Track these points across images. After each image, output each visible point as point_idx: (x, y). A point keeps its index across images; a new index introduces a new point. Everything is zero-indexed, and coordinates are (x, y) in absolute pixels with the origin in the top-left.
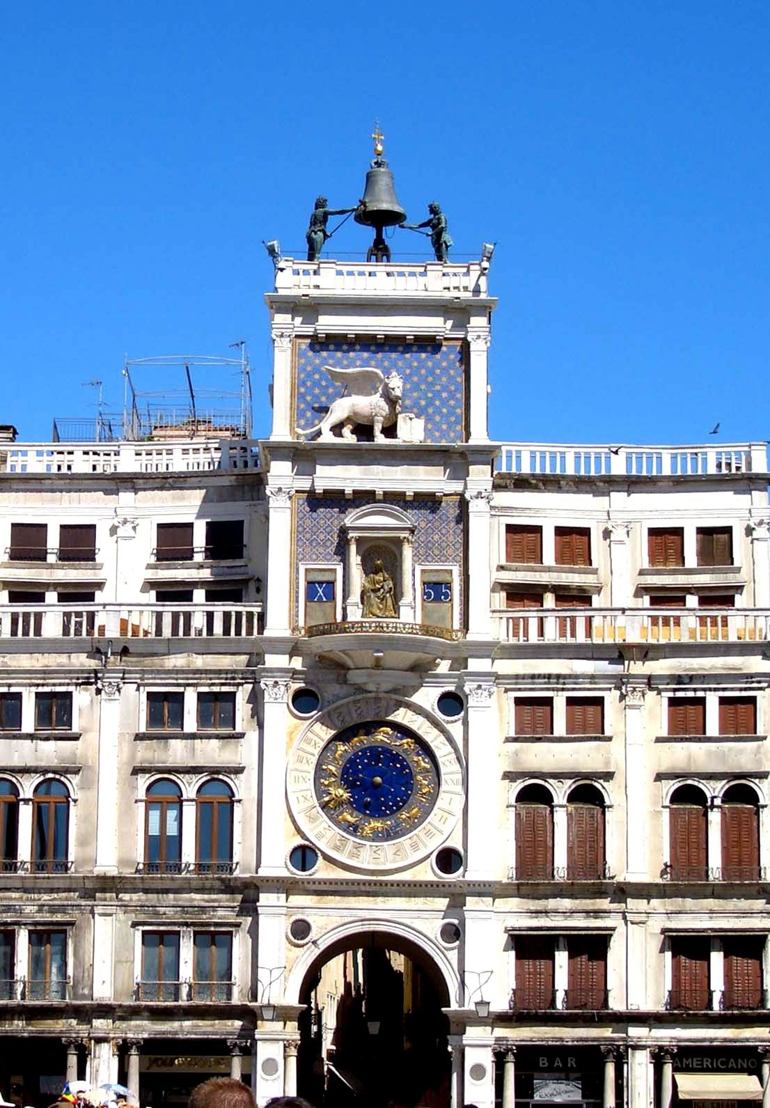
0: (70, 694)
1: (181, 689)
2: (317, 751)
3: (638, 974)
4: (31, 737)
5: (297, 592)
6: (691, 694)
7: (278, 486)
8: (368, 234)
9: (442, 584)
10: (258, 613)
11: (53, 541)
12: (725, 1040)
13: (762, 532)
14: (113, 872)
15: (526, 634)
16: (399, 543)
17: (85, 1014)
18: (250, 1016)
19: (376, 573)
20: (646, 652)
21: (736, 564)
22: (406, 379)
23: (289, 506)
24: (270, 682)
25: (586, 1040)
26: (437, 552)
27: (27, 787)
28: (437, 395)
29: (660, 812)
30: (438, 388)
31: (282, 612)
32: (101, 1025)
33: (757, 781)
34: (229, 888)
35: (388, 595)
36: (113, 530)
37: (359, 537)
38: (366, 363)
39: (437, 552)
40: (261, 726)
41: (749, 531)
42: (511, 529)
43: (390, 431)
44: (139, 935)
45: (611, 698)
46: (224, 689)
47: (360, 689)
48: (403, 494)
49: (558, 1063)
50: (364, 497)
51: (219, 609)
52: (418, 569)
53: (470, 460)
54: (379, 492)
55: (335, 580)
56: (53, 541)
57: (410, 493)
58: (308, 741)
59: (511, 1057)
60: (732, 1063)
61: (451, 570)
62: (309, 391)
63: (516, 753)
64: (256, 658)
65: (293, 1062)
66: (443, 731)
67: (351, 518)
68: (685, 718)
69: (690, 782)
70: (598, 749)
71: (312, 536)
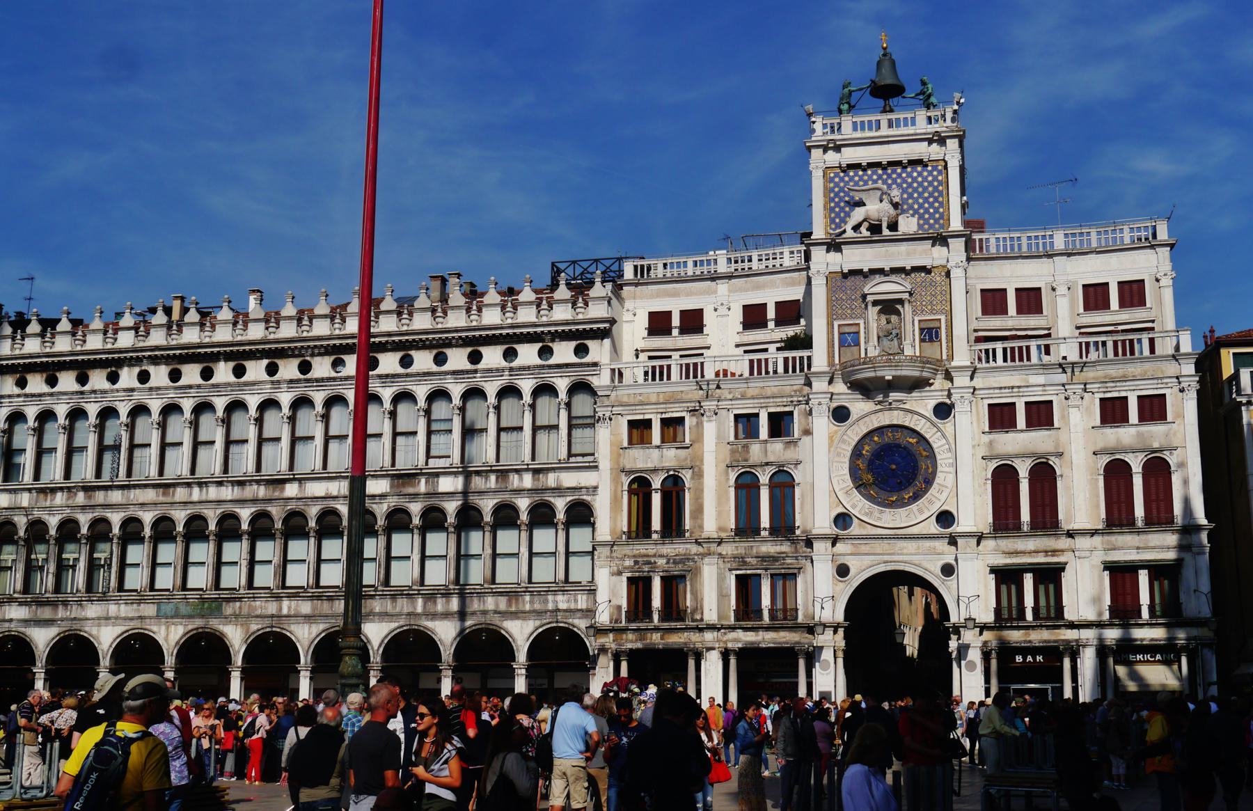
0: (683, 418)
1: (756, 411)
2: (850, 449)
6: (1115, 395)
8: (881, 102)
11: (676, 321)
12: (1152, 640)
13: (1166, 282)
15: (995, 360)
21: (1148, 305)
22: (904, 191)
24: (816, 402)
25: (1049, 641)
27: (656, 483)
28: (926, 200)
29: (1097, 480)
30: (926, 195)
31: (819, 356)
32: (709, 636)
33: (1167, 453)
38: (875, 182)
43: (893, 226)
44: (733, 578)
46: (787, 409)
49: (1029, 659)
51: (781, 356)
52: (917, 319)
54: (887, 269)
56: (676, 321)
57: (908, 268)
58: (844, 441)
59: (994, 655)
60: (1158, 657)
62: (837, 205)
63: (991, 443)
65: (840, 661)
66: (939, 430)
68: (1113, 412)
69: (1118, 457)
70: (1049, 436)
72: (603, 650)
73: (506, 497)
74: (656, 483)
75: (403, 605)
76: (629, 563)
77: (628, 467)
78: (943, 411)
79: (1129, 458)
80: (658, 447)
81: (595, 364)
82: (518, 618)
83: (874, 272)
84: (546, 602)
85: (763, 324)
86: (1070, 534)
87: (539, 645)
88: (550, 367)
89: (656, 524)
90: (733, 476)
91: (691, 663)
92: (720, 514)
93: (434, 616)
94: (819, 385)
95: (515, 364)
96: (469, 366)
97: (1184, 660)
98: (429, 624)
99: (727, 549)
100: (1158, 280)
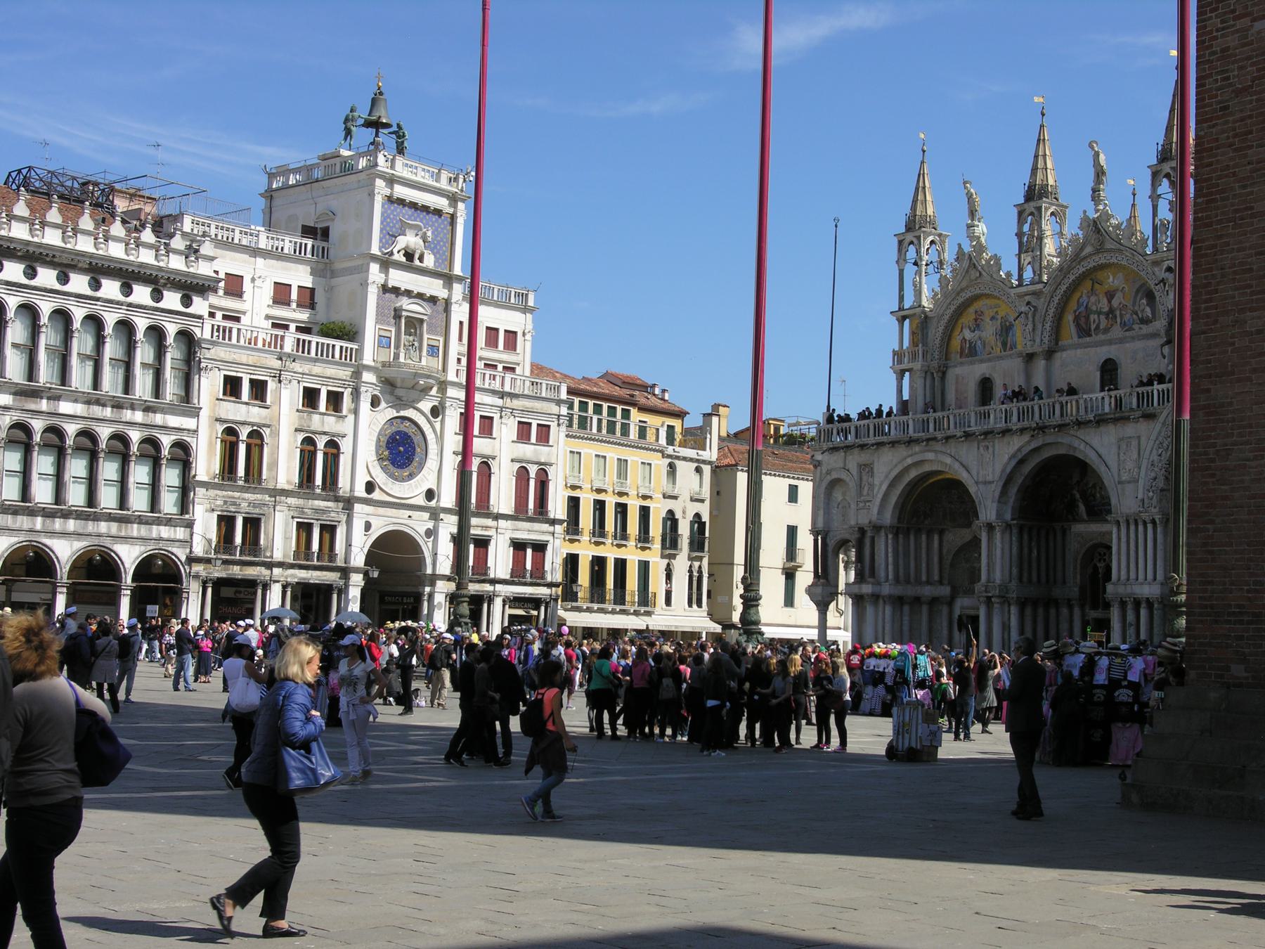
3: (500, 561)
4: (246, 403)
13: (528, 337)
14: (286, 487)
17: (270, 565)
18: (345, 572)
20: (513, 396)
27: (244, 433)
32: (276, 571)
34: (337, 499)
36: (253, 280)
40: (356, 412)
41: (524, 334)
43: (421, 259)
45: (496, 417)
47: (399, 398)
50: (408, 293)
64: (357, 374)
68: (523, 431)
72: (197, 577)
73: (121, 427)
74: (244, 433)
75: (23, 522)
76: (219, 502)
77: (223, 416)
78: (435, 412)
79: (529, 467)
80: (246, 403)
81: (200, 317)
82: (127, 543)
84: (150, 531)
85: (287, 303)
86: (497, 517)
87: (144, 568)
88: (163, 311)
89: (241, 471)
90: (301, 436)
91: (259, 592)
92: (288, 468)
93: (53, 534)
94: (368, 377)
95: (130, 299)
96: (88, 291)
97: (543, 609)
98: (48, 541)
99: (292, 501)
100: (524, 334)
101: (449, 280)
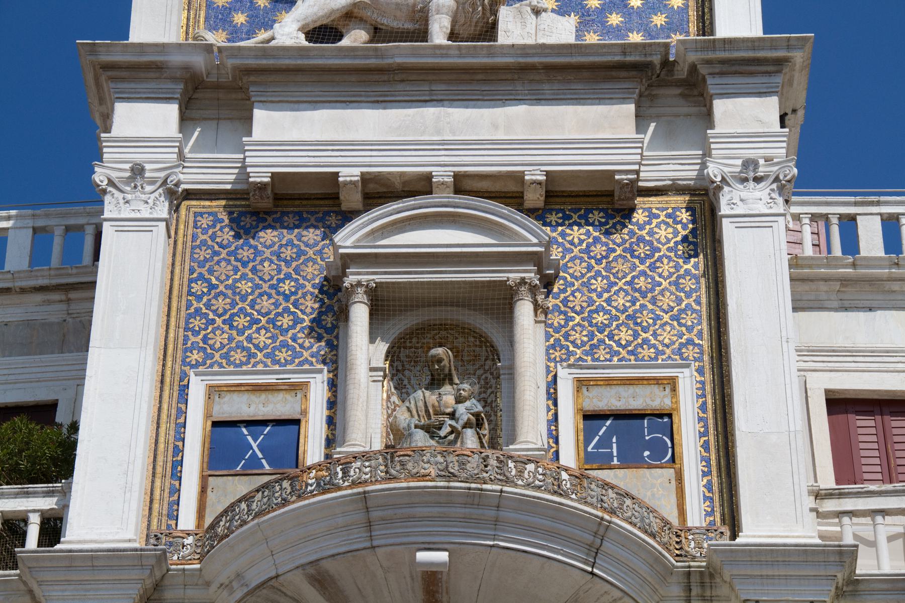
5: (178, 451)
7: (127, 166)
9: (640, 416)
10: (42, 513)
16: (501, 302)
19: (436, 381)
23: (165, 215)
26: (624, 335)
35: (470, 433)
37: (379, 285)
39: (624, 335)
42: (838, 404)
48: (518, 178)
53: (712, 90)
54: (442, 175)
55: (304, 412)
57: (535, 175)
61: (672, 384)
67: (350, 238)
71: (233, 304)
83: (378, 191)
101: (671, 83)
